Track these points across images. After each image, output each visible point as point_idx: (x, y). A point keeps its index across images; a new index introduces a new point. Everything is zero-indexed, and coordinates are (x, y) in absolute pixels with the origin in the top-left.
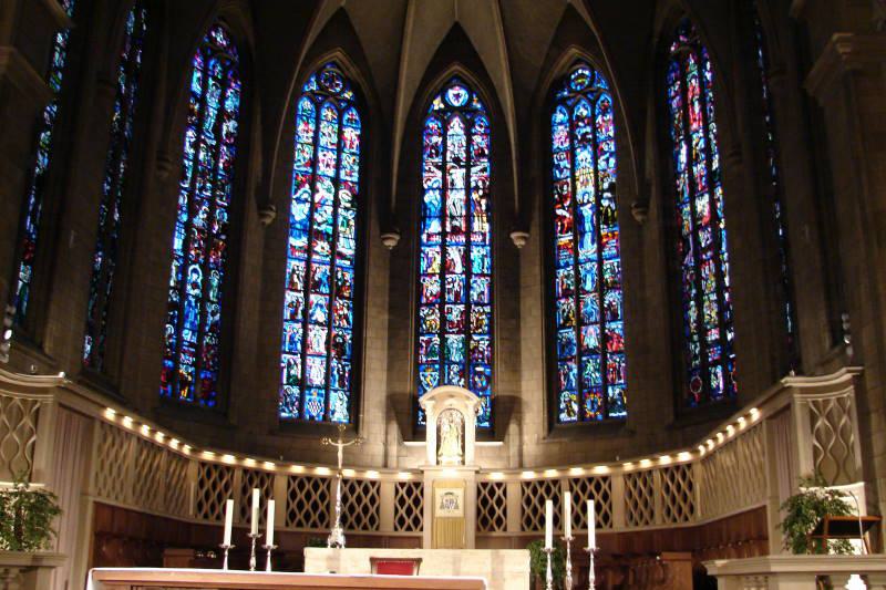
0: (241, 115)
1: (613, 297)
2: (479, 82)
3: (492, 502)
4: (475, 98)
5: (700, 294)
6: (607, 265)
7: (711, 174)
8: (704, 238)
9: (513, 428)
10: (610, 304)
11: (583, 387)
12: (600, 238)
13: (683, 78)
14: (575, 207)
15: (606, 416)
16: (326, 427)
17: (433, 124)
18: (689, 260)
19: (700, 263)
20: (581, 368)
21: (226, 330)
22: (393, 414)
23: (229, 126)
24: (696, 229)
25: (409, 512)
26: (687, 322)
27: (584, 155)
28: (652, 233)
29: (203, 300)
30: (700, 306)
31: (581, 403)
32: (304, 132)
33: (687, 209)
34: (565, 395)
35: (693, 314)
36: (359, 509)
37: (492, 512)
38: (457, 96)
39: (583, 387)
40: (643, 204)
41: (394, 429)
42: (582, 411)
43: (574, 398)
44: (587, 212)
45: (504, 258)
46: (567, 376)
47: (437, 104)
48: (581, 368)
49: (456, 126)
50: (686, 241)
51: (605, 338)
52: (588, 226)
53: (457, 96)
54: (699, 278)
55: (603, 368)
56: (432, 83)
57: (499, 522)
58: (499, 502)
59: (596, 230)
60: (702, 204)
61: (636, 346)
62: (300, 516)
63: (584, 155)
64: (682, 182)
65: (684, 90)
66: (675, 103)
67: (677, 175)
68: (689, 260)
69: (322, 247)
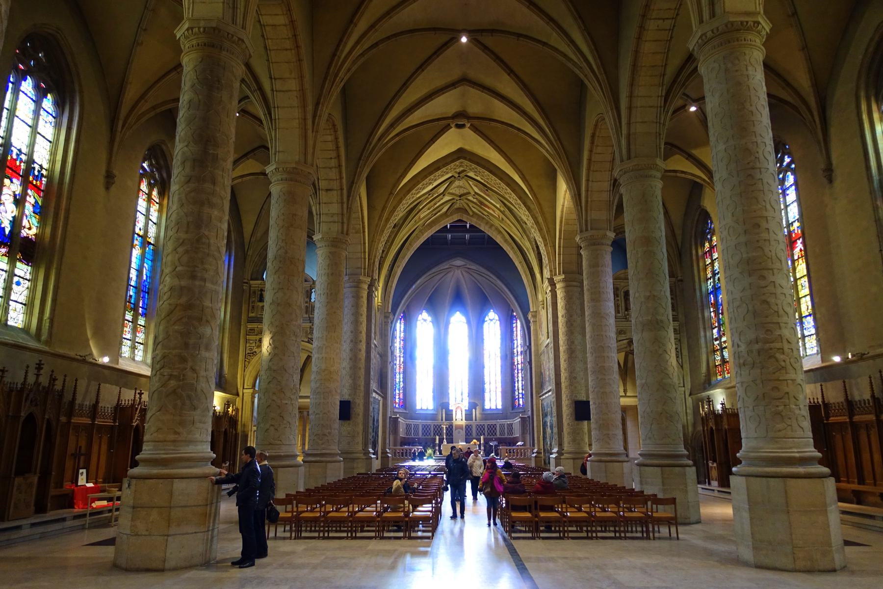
0: (405, 331)
3: (469, 429)
5: (518, 381)
7: (521, 352)
8: (520, 367)
13: (516, 322)
18: (516, 371)
19: (518, 373)
21: (404, 388)
23: (402, 335)
24: (518, 364)
25: (449, 432)
26: (515, 386)
29: (400, 382)
30: (518, 383)
33: (516, 358)
35: (516, 385)
36: (437, 432)
37: (469, 432)
54: (518, 377)
57: (471, 434)
58: (471, 429)
60: (519, 358)
62: (425, 434)
64: (515, 351)
65: (517, 327)
66: (515, 329)
67: (514, 349)
68: (516, 371)
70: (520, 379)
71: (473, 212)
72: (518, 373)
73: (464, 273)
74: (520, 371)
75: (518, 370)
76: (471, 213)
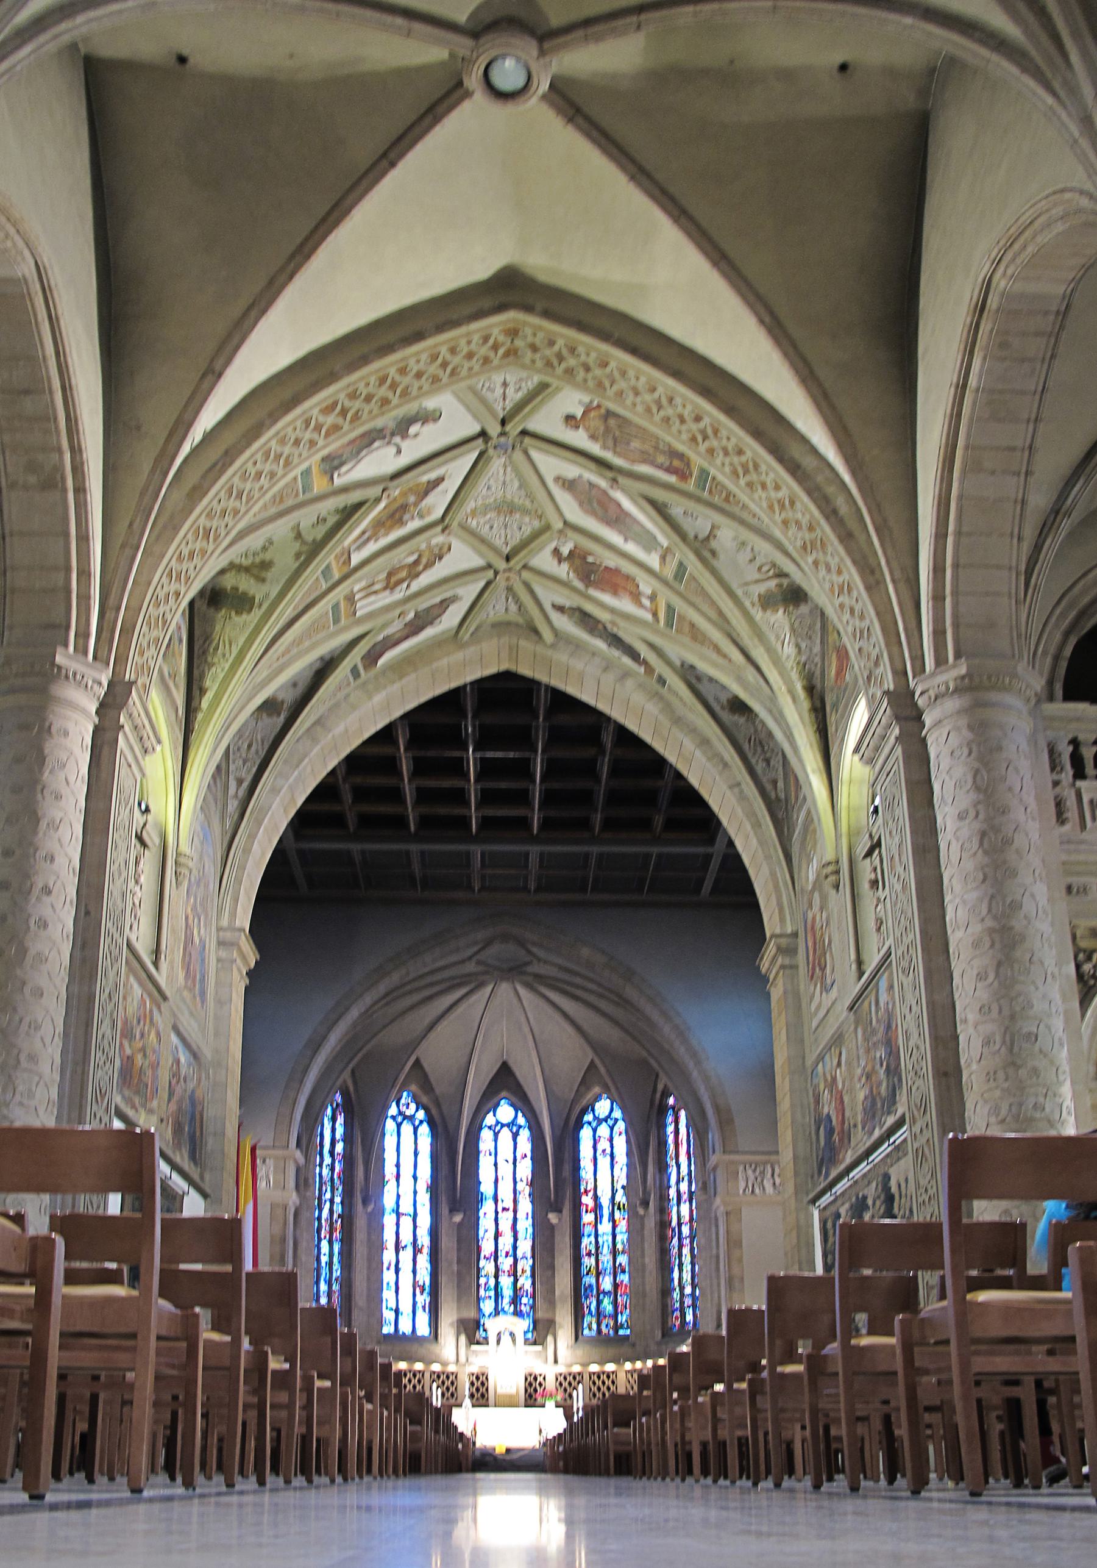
1: (623, 1259)
2: (523, 1102)
4: (520, 1114)
6: (619, 1238)
9: (550, 1339)
10: (620, 1264)
11: (599, 1315)
12: (614, 1222)
14: (596, 1198)
15: (616, 1332)
16: (414, 1337)
17: (486, 1135)
18: (675, 1241)
20: (599, 1302)
22: (462, 1329)
27: (604, 1162)
28: (651, 1223)
31: (599, 1324)
32: (390, 1142)
34: (587, 1319)
38: (505, 1112)
39: (599, 1315)
40: (645, 1204)
41: (463, 1339)
42: (599, 1331)
43: (594, 1320)
44: (605, 1202)
45: (543, 1236)
46: (589, 1307)
47: (490, 1120)
48: (599, 1302)
49: (505, 1135)
50: (673, 1230)
51: (616, 1286)
52: (606, 1213)
53: (505, 1112)
55: (615, 1303)
56: (487, 1101)
59: (612, 1214)
61: (637, 1293)
63: (604, 1162)
68: (675, 1241)
69: (406, 1223)
70: (687, 1260)
71: (556, 632)
72: (681, 1246)
73: (522, 991)
74: (687, 1242)
75: (680, 1239)
76: (547, 635)
